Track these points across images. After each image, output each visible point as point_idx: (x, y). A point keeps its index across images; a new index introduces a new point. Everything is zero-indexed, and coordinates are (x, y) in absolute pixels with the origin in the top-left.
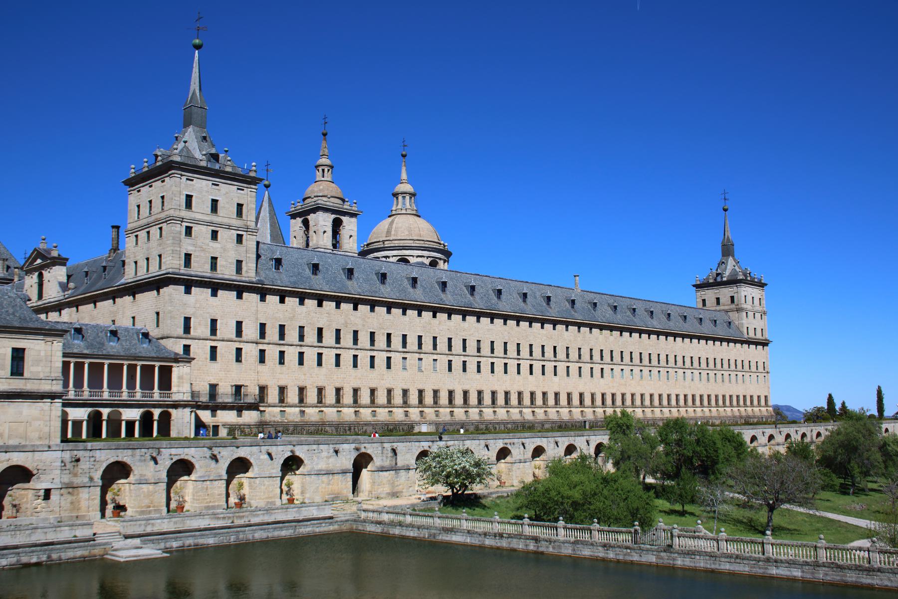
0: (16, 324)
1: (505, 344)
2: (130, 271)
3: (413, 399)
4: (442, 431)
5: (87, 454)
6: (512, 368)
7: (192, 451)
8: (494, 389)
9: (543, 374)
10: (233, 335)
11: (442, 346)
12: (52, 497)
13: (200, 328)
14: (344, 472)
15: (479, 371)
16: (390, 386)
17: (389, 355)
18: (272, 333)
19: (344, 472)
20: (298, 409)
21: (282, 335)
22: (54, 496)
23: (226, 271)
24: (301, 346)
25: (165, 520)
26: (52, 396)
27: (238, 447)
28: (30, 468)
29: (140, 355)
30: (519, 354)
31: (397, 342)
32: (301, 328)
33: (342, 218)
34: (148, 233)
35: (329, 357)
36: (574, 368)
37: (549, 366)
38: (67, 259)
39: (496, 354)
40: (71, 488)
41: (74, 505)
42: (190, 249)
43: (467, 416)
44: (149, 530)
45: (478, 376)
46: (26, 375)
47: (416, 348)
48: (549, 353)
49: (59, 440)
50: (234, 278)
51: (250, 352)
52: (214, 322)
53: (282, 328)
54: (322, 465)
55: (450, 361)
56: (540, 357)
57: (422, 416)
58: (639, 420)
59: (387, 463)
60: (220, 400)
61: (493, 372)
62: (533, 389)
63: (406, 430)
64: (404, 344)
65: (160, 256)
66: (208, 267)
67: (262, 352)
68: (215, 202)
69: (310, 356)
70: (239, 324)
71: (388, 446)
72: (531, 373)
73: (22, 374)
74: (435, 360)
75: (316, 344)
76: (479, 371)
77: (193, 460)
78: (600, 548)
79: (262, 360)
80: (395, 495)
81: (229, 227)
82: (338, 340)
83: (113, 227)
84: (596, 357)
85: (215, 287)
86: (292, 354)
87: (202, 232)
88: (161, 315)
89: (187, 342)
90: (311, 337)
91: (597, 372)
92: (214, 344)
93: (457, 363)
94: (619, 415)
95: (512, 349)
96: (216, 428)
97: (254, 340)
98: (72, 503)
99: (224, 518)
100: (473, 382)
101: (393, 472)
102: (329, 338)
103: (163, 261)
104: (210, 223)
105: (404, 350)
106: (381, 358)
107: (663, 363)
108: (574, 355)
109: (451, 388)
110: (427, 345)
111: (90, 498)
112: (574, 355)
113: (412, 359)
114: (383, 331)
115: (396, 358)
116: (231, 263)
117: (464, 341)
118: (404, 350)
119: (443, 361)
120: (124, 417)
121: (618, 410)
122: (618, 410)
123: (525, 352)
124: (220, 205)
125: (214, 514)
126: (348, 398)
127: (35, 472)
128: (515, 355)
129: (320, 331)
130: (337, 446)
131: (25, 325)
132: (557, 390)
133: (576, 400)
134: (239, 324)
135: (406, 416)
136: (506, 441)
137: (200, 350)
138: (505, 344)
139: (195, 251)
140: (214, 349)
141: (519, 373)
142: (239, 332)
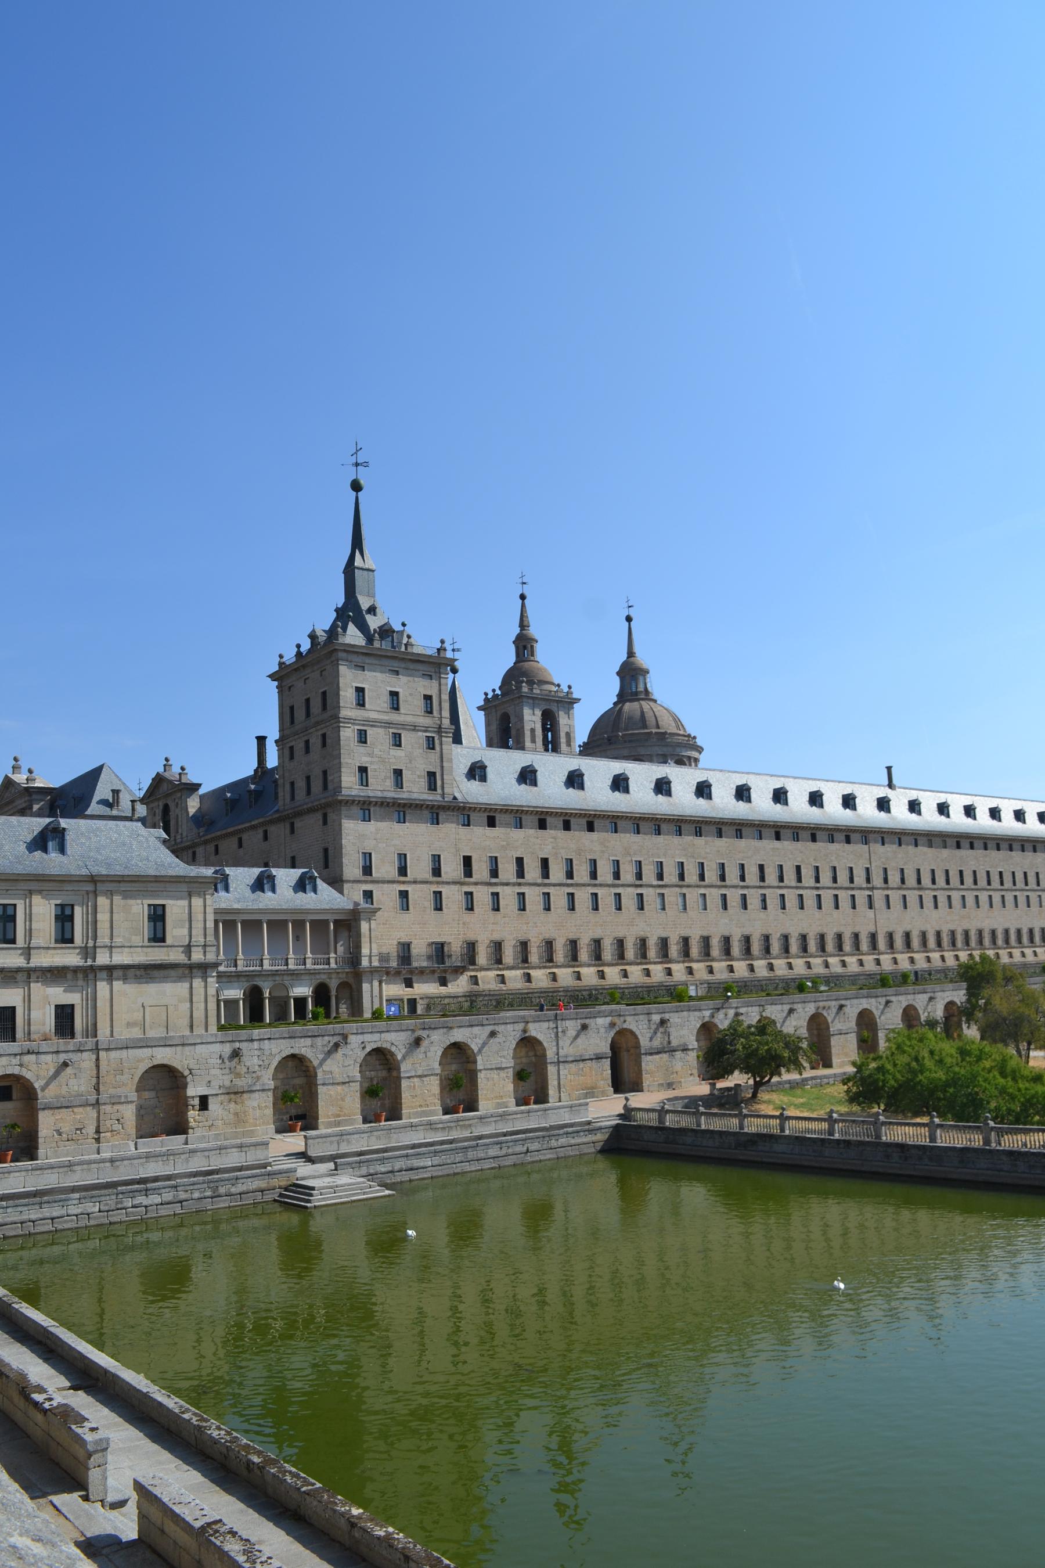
0: (152, 872)
1: (798, 868)
2: (284, 793)
4: (721, 992)
5: (256, 1045)
6: (810, 902)
7: (391, 1037)
8: (785, 932)
9: (854, 907)
10: (428, 875)
11: (711, 876)
12: (210, 1107)
13: (384, 867)
14: (598, 1058)
15: (765, 908)
17: (639, 891)
18: (480, 870)
19: (598, 1058)
20: (519, 973)
21: (494, 873)
22: (212, 1104)
23: (415, 788)
24: (520, 884)
25: (366, 1135)
26: (204, 968)
27: (451, 1028)
28: (179, 1068)
29: (308, 907)
30: (817, 880)
31: (649, 874)
32: (520, 861)
33: (554, 707)
34: (307, 742)
35: (559, 899)
36: (895, 896)
37: (861, 897)
38: (200, 785)
39: (786, 882)
40: (234, 1093)
41: (239, 1119)
42: (365, 761)
44: (344, 1149)
45: (762, 914)
46: (169, 940)
48: (860, 879)
49: (215, 1028)
50: (425, 797)
51: (452, 896)
52: (402, 857)
53: (494, 860)
54: (567, 1049)
55: (724, 897)
56: (847, 884)
58: (1004, 967)
59: (657, 1043)
60: (415, 964)
61: (784, 908)
62: (842, 929)
63: (676, 995)
64: (660, 876)
65: (325, 773)
66: (389, 783)
67: (469, 895)
68: (394, 695)
69: (534, 896)
70: (437, 859)
71: (656, 1018)
72: (837, 907)
73: (163, 940)
74: (704, 895)
75: (540, 881)
77: (393, 1049)
78: (1004, 1158)
79: (470, 908)
80: (670, 1086)
81: (415, 728)
82: (570, 875)
83: (258, 738)
84: (926, 880)
85: (401, 810)
86: (508, 896)
87: (378, 737)
88: (330, 852)
89: (368, 887)
90: (533, 872)
91: (928, 902)
92: (403, 888)
93: (734, 897)
94: (977, 959)
95: (807, 874)
96: (412, 1003)
97: (457, 879)
98: (236, 1114)
99: (444, 1128)
100: (756, 923)
101: (665, 1056)
102: (557, 873)
103: (330, 778)
104: (388, 724)
105: (660, 883)
106: (628, 896)
107: (1020, 883)
108: (894, 879)
109: (727, 934)
110: (692, 876)
111: (261, 1107)
112: (894, 879)
113: (672, 896)
116: (419, 777)
117: (742, 866)
118: (660, 883)
119: (714, 896)
120: (291, 994)
121: (977, 954)
122: (977, 954)
123: (826, 878)
124: (401, 696)
125: (430, 1124)
127: (186, 1072)
128: (812, 883)
129: (545, 863)
130: (587, 1021)
131: (163, 873)
132: (873, 930)
133: (899, 942)
134: (437, 859)
136: (821, 1004)
137: (386, 896)
138: (798, 868)
139: (372, 763)
140: (404, 895)
141: (820, 908)
142: (437, 872)
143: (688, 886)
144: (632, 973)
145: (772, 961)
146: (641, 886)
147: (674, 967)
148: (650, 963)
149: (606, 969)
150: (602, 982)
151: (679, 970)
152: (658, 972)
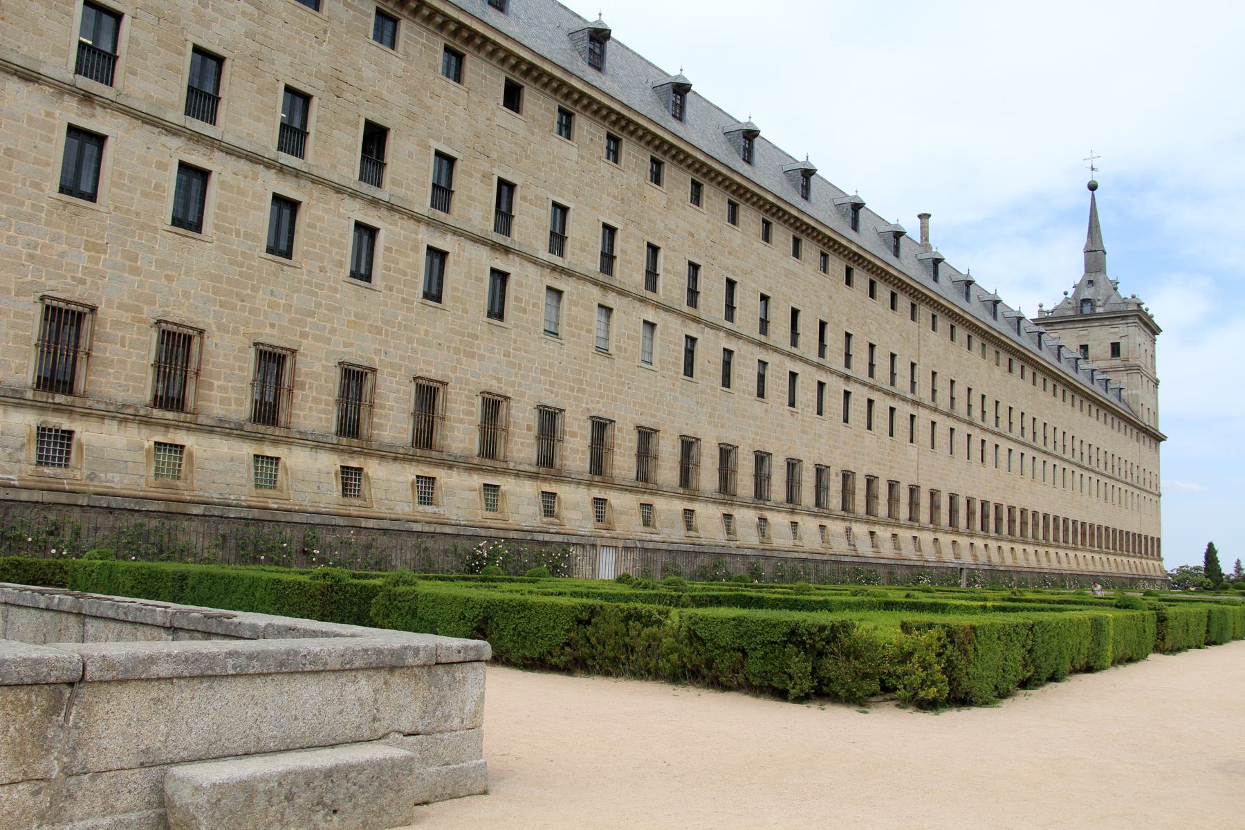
3: (575, 450)
16: (495, 387)
43: (729, 531)
45: (757, 406)
47: (592, 265)
57: (600, 518)
74: (651, 326)
76: (761, 394)
106: (469, 268)
113: (581, 300)
114: (484, 165)
115: (527, 284)
119: (673, 331)
126: (314, 406)
135: (549, 512)
138: (822, 325)
143: (622, 293)
144: (451, 493)
145: (768, 515)
146: (507, 250)
147: (566, 493)
148: (505, 472)
149: (374, 469)
150: (354, 507)
151: (576, 504)
152: (521, 503)
